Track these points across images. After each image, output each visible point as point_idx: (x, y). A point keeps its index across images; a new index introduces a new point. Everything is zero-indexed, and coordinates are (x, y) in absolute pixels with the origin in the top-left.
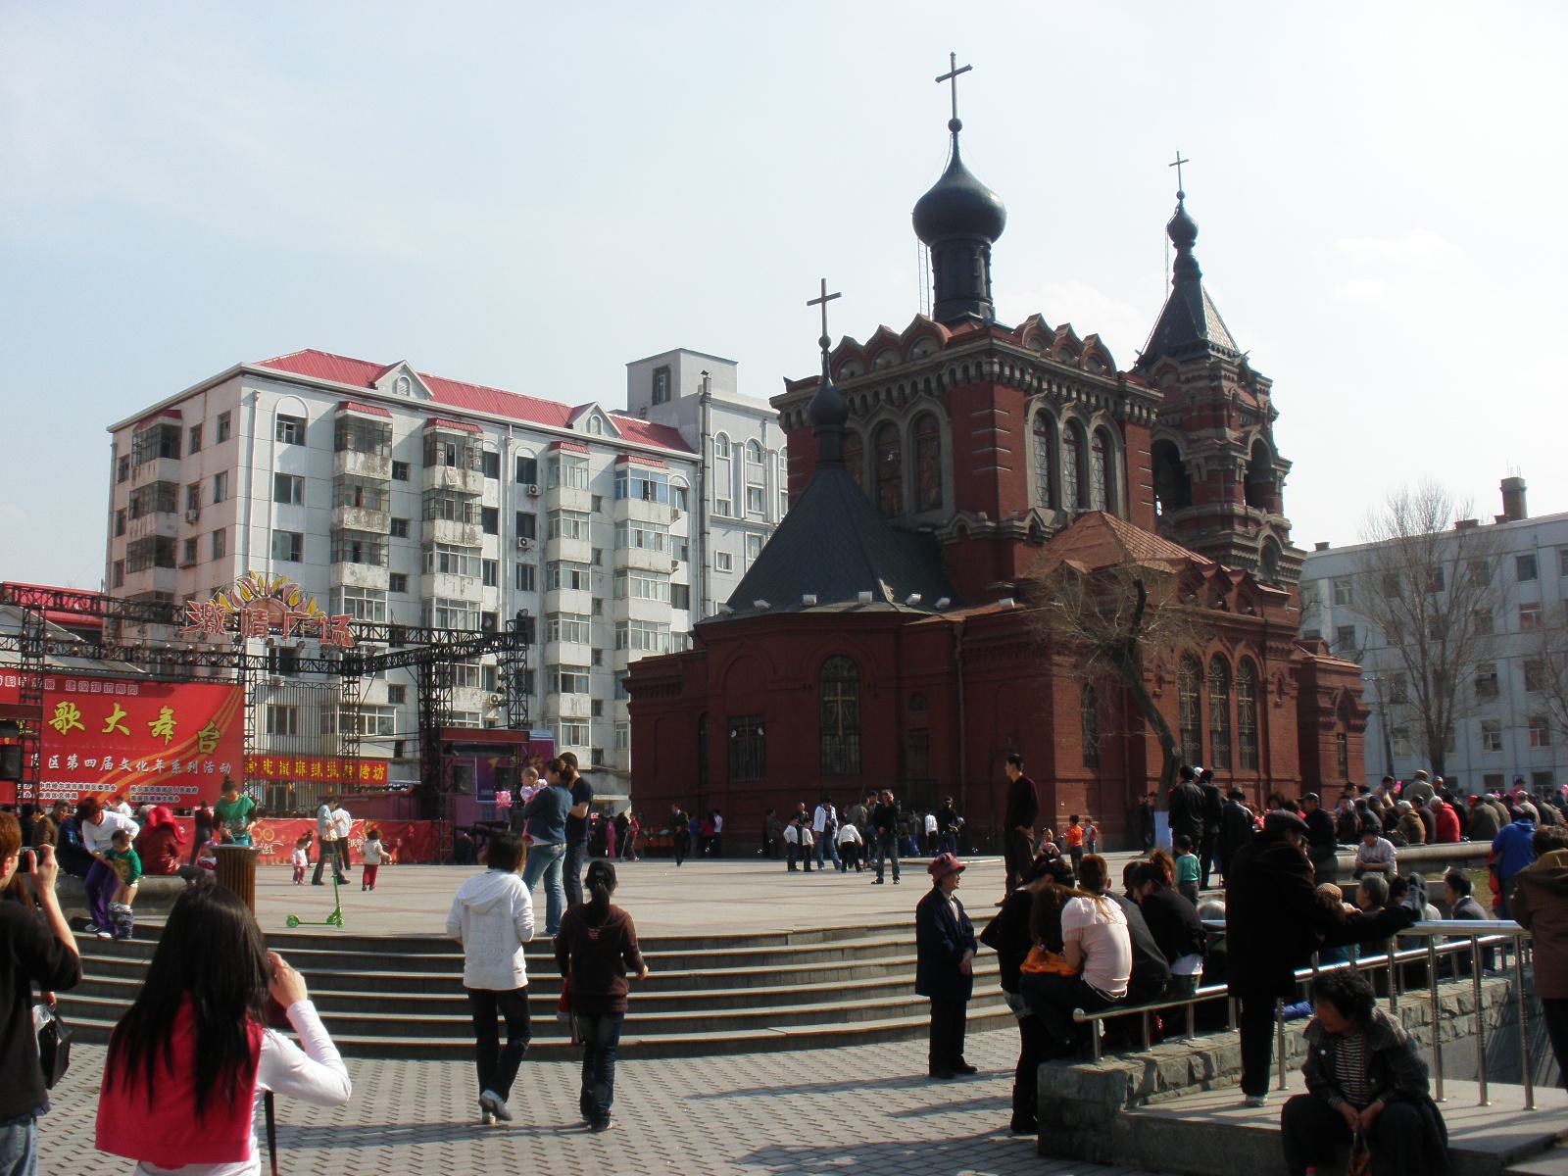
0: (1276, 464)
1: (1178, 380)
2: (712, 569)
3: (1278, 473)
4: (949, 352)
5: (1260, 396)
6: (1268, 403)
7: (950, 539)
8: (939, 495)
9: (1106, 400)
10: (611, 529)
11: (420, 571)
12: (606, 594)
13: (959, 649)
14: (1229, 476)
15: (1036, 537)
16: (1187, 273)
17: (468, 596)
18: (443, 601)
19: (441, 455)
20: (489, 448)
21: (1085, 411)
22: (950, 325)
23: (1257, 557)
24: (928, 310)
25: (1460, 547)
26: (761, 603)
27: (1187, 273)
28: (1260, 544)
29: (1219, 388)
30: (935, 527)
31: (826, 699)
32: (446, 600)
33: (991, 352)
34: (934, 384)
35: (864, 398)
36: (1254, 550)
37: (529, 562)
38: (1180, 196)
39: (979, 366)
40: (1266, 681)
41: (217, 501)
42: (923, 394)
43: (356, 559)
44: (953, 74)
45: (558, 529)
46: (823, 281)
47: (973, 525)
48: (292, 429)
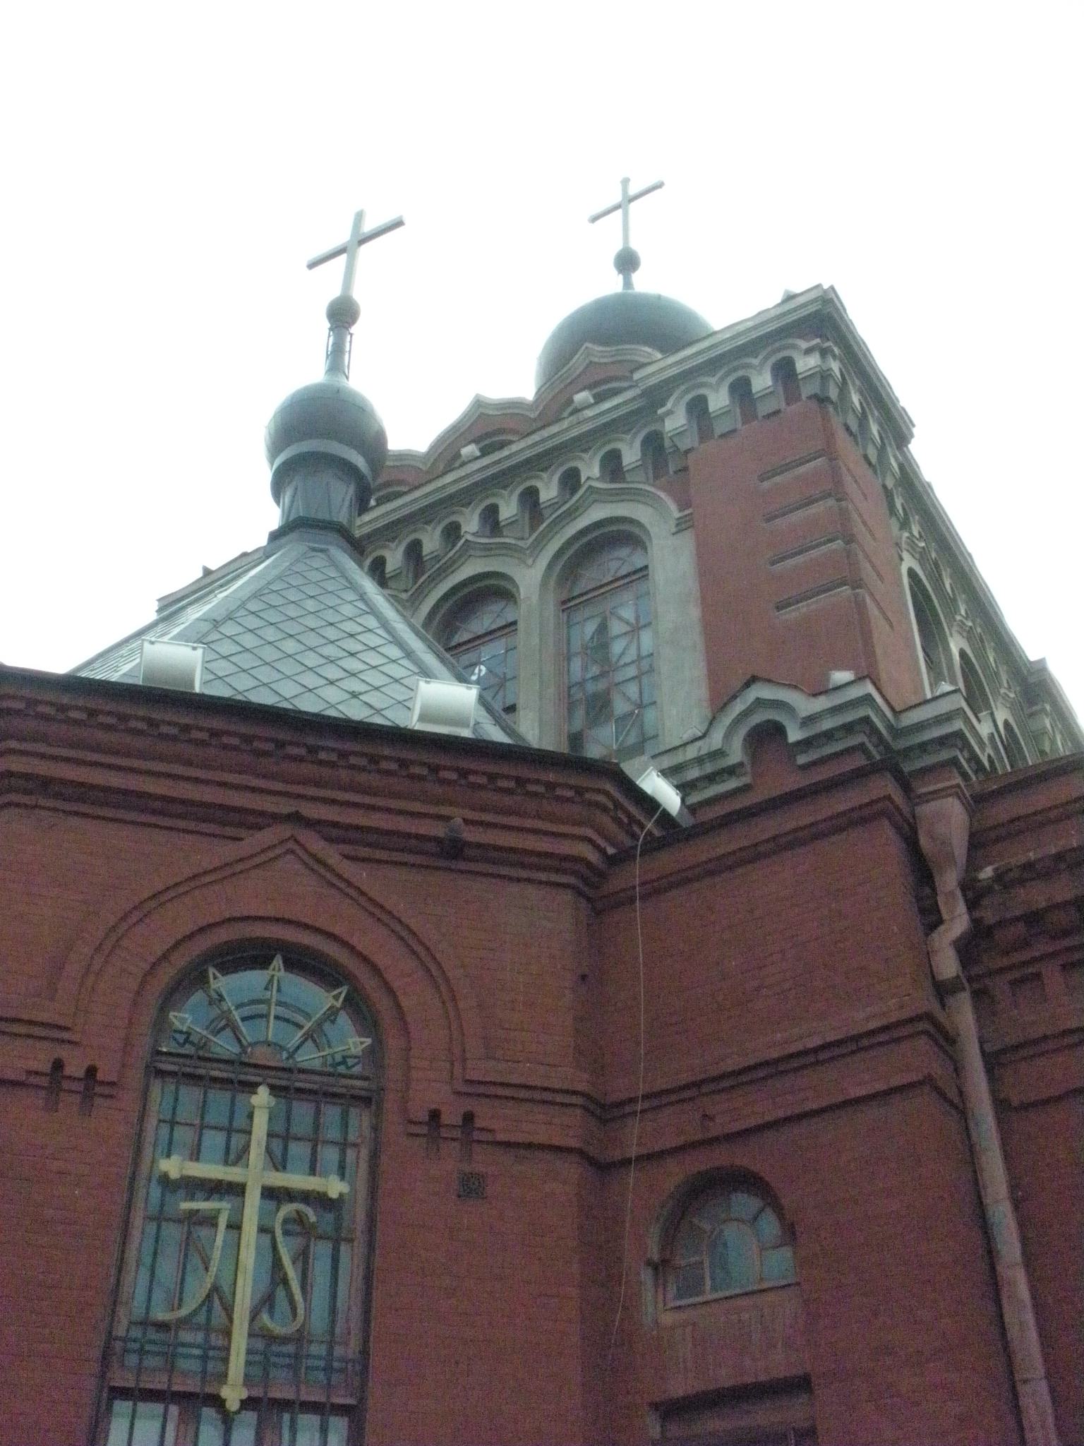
7: (711, 778)
13: (957, 922)
31: (173, 1166)
47: (806, 705)
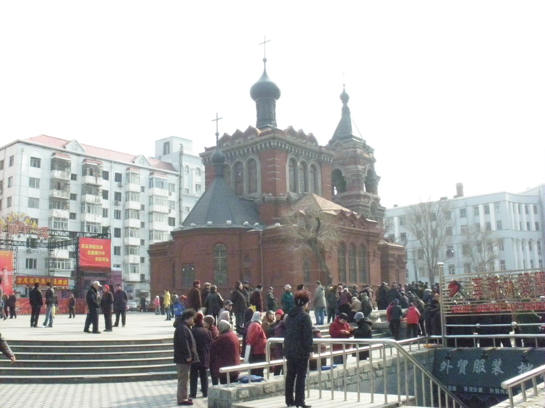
0: (375, 177)
1: (342, 149)
2: (183, 212)
3: (377, 181)
4: (260, 138)
5: (370, 154)
6: (373, 156)
8: (256, 187)
9: (315, 155)
10: (148, 198)
11: (80, 212)
12: (146, 220)
13: (261, 240)
14: (359, 181)
15: (289, 202)
16: (346, 111)
17: (97, 221)
18: (87, 222)
19: (88, 172)
20: (105, 169)
21: (308, 158)
22: (260, 129)
23: (369, 209)
24: (254, 125)
25: (440, 206)
26: (193, 224)
27: (346, 111)
28: (369, 205)
29: (356, 151)
30: (254, 198)
31: (215, 257)
32: (89, 222)
33: (274, 138)
34: (255, 149)
35: (231, 154)
36: (368, 207)
37: (119, 209)
38: (344, 85)
39: (270, 143)
40: (369, 252)
41: (9, 187)
42: (251, 153)
43: (59, 208)
44: (265, 42)
45: (129, 198)
46: (217, 113)
48: (36, 162)
